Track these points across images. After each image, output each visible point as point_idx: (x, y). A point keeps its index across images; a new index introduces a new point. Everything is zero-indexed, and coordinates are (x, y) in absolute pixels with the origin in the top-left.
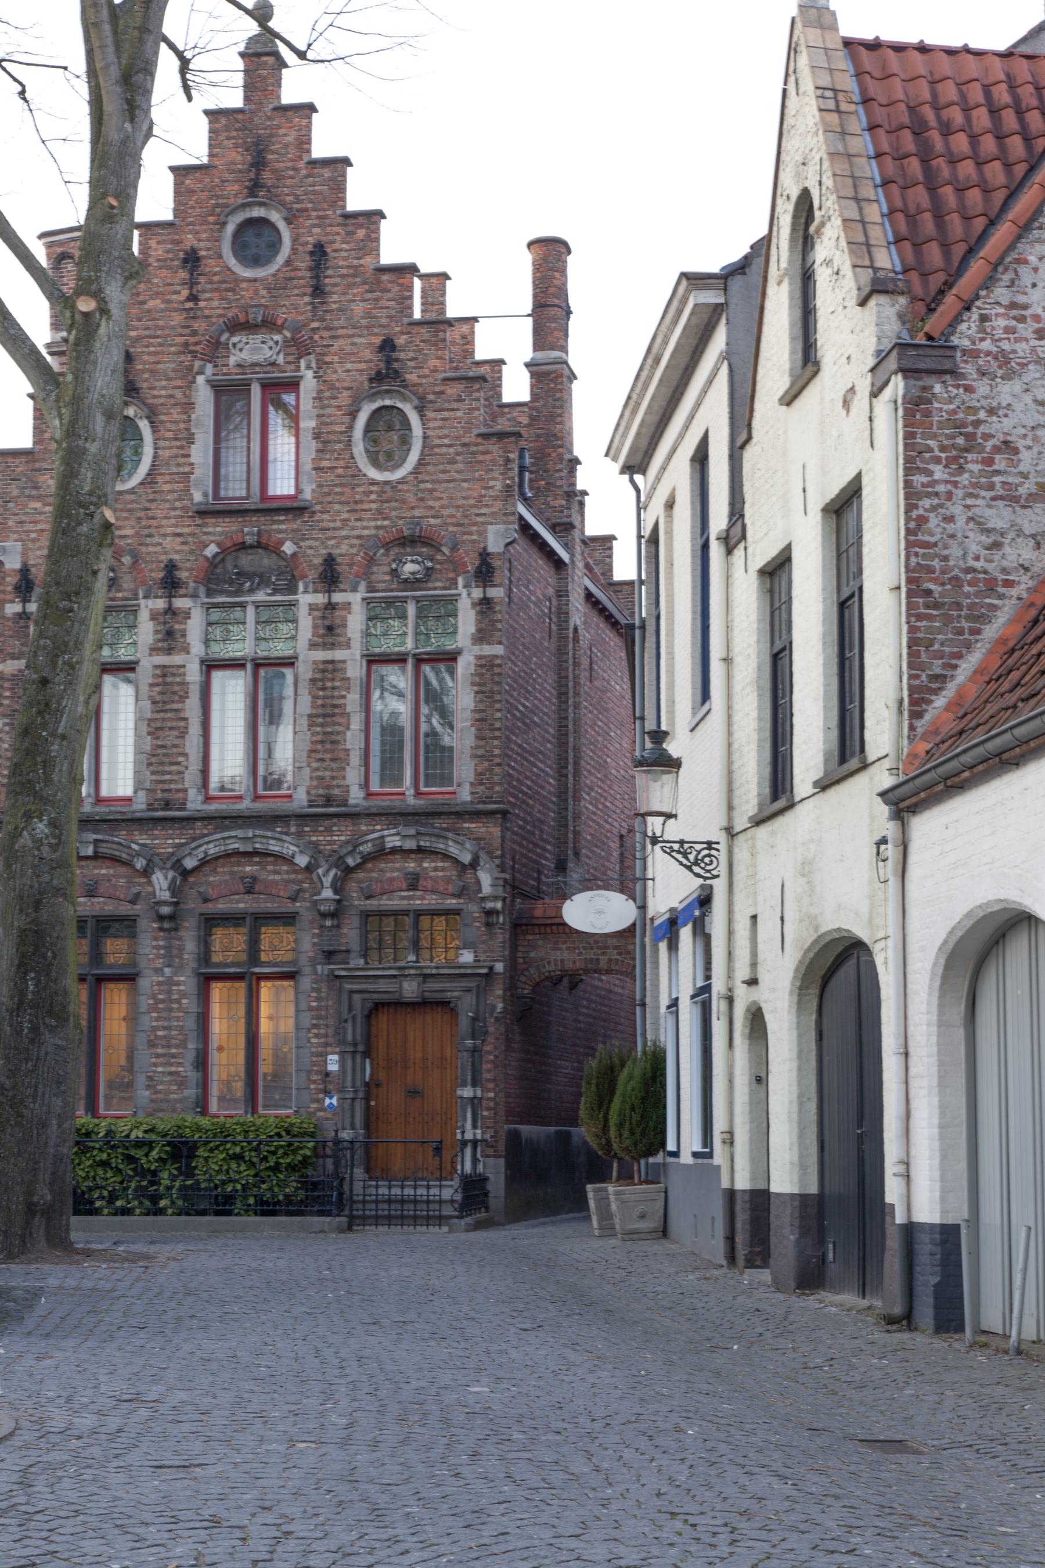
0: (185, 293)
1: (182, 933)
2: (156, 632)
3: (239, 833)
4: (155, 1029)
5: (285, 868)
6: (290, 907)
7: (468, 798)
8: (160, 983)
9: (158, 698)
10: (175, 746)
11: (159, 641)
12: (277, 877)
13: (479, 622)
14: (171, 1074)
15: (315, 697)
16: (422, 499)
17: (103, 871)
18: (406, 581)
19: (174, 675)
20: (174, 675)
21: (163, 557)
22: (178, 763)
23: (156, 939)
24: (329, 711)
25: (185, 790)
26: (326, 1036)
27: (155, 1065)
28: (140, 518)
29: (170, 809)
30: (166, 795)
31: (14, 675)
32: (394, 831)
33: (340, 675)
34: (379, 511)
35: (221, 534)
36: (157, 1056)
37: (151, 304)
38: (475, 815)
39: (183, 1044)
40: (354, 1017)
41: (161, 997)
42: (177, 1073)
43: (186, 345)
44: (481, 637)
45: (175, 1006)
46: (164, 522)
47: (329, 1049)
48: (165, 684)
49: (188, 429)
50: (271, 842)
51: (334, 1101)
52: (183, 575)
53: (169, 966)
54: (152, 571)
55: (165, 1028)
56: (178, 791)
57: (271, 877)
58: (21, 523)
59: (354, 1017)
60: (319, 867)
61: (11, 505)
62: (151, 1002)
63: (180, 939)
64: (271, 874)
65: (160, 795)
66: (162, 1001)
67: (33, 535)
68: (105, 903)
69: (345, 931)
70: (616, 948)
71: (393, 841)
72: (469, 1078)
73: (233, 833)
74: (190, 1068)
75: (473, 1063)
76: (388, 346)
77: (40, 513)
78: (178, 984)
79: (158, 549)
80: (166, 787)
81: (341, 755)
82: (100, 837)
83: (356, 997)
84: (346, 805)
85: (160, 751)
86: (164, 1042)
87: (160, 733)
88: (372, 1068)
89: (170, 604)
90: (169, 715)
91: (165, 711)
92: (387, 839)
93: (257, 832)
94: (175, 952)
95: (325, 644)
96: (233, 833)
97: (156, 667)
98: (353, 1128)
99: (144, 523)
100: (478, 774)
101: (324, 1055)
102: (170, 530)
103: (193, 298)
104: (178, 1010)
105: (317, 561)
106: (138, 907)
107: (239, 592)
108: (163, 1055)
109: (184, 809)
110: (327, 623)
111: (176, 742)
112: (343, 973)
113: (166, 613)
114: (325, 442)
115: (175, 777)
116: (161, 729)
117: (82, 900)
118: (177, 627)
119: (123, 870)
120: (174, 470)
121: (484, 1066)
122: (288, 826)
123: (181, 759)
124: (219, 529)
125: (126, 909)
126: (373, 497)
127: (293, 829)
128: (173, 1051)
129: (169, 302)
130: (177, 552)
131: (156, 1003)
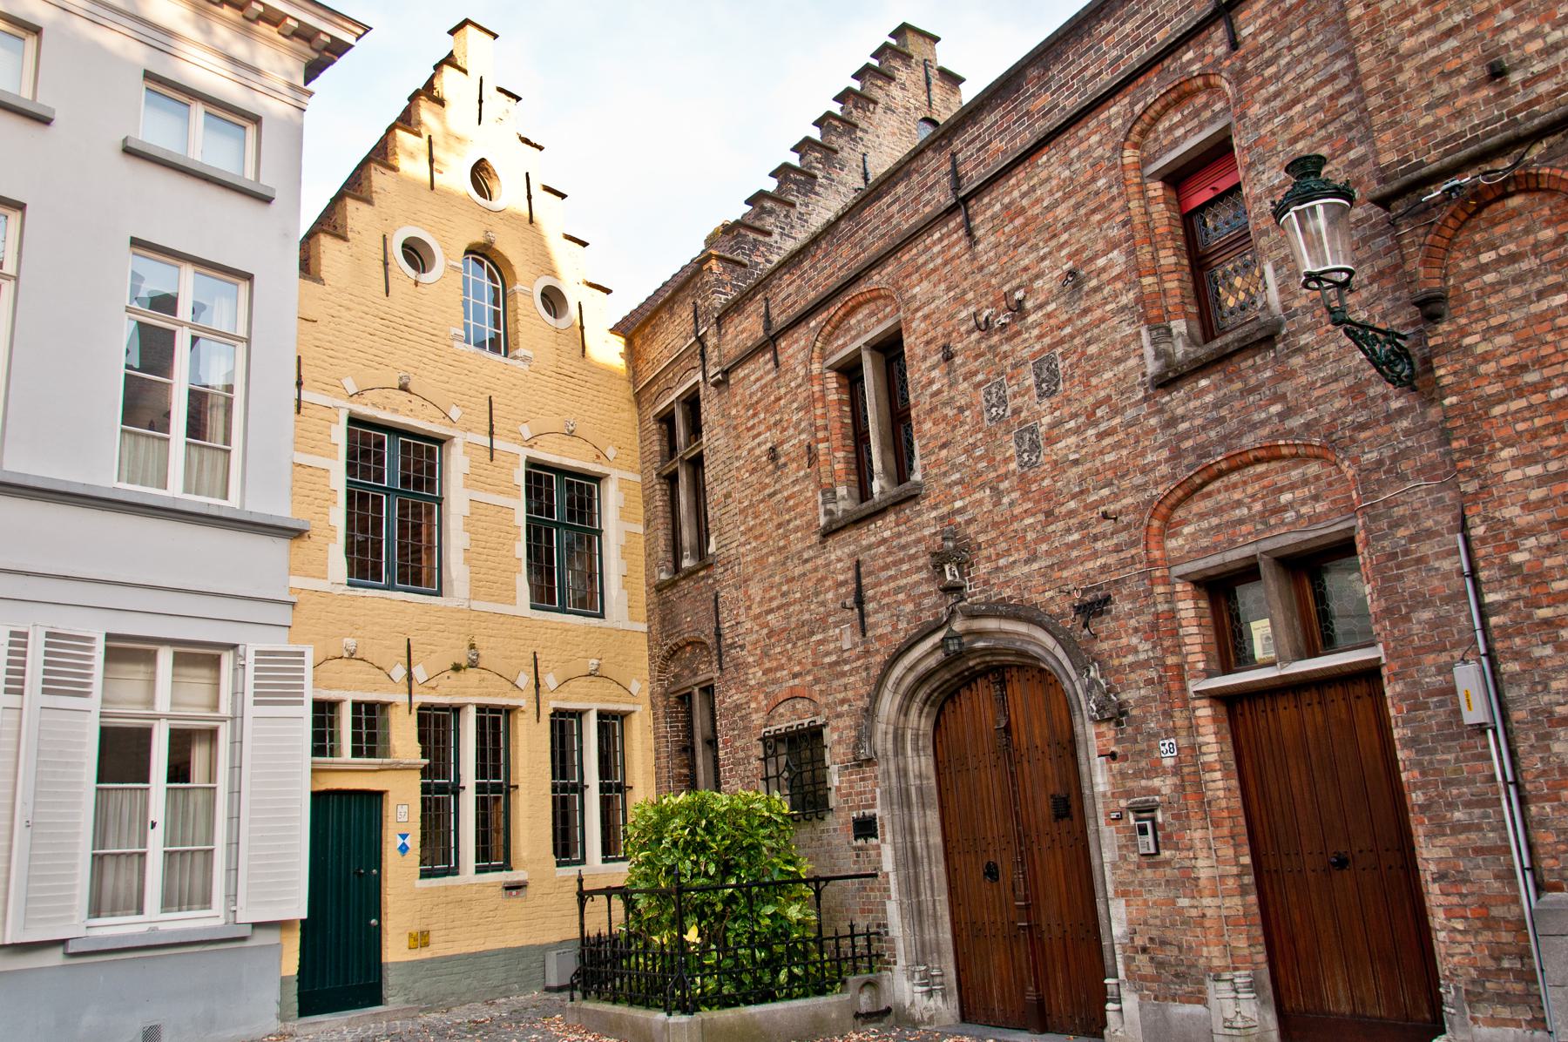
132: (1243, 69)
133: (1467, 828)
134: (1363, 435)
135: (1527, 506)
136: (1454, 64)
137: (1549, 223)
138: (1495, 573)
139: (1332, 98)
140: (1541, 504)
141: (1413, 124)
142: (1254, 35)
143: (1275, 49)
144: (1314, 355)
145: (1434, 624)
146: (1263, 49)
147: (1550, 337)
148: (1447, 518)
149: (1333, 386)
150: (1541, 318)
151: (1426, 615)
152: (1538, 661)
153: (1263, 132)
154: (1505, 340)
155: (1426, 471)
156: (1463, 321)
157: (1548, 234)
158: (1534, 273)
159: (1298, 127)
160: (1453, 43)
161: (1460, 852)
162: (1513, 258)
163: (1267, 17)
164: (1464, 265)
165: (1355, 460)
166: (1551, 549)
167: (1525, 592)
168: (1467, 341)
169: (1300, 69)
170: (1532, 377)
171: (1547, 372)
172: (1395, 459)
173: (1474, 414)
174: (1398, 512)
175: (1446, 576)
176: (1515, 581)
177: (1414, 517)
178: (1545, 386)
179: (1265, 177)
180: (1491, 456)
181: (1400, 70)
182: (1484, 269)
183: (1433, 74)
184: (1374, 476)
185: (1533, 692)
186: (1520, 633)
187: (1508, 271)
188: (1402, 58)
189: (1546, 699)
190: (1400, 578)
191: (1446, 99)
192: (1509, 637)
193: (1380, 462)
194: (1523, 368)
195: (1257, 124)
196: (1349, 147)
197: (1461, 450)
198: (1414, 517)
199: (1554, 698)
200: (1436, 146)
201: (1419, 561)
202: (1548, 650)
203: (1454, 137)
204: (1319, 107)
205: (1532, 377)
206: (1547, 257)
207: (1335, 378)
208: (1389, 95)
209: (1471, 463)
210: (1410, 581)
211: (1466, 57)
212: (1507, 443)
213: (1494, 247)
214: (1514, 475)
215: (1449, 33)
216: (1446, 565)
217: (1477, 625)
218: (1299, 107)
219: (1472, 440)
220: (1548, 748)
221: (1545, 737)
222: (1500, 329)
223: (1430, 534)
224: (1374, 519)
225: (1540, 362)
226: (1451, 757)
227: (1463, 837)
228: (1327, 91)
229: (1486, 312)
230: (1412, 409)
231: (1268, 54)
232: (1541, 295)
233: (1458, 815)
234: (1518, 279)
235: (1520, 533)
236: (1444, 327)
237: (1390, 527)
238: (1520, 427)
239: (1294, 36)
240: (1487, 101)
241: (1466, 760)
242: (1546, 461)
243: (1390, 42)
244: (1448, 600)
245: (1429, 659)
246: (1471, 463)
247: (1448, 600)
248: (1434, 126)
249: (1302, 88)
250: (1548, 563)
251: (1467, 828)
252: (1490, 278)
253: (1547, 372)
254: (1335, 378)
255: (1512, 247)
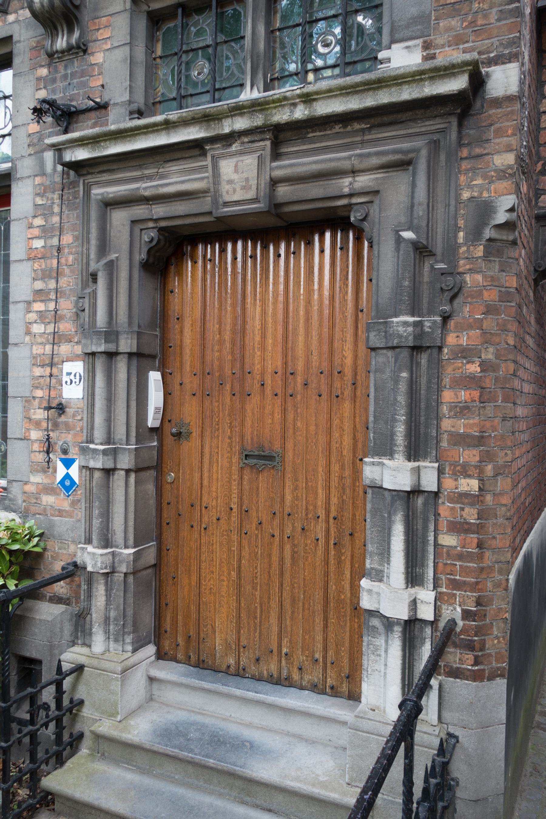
26: (57, 317)
40: (111, 266)
47: (64, 349)
51: (74, 471)
59: (111, 266)
69: (98, 58)
72: (400, 429)
75: (412, 384)
88: (167, 394)
98: (106, 543)
121: (448, 396)
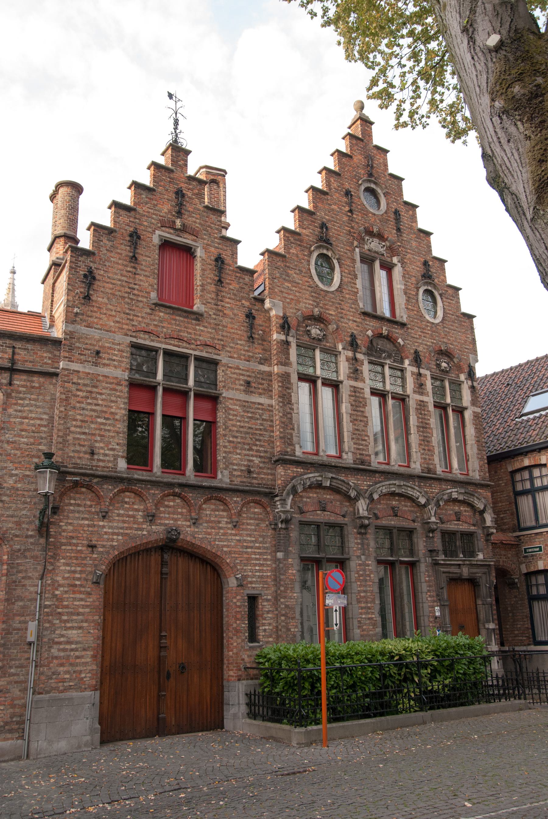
0: (347, 209)
1: (368, 536)
2: (349, 368)
3: (397, 482)
4: (359, 592)
5: (409, 504)
6: (412, 525)
7: (478, 478)
8: (360, 565)
9: (353, 403)
10: (363, 431)
11: (351, 373)
12: (406, 508)
13: (472, 396)
14: (369, 619)
15: (418, 417)
16: (446, 335)
17: (328, 497)
18: (443, 371)
19: (359, 393)
20: (359, 393)
21: (349, 330)
22: (365, 440)
23: (356, 539)
24: (424, 425)
25: (370, 456)
27: (361, 614)
28: (337, 308)
29: (364, 465)
30: (361, 457)
31: (282, 374)
32: (456, 490)
33: (426, 408)
34: (431, 335)
35: (373, 326)
36: (362, 608)
37: (333, 207)
38: (482, 486)
39: (373, 601)
41: (361, 573)
42: (372, 618)
43: (350, 231)
44: (474, 402)
45: (368, 578)
46: (348, 313)
48: (356, 396)
49: (354, 271)
50: (409, 489)
52: (359, 342)
53: (363, 555)
54: (345, 336)
55: (365, 591)
56: (367, 455)
57: (404, 508)
58: (282, 292)
60: (429, 504)
61: (275, 280)
62: (356, 575)
63: (367, 539)
64: (405, 507)
65: (359, 457)
66: (362, 575)
67: (288, 300)
68: (330, 516)
70: (504, 555)
71: (455, 495)
73: (394, 482)
74: (378, 615)
76: (425, 263)
77: (291, 290)
78: (368, 565)
79: (346, 325)
80: (361, 452)
81: (432, 448)
82: (334, 476)
83: (444, 575)
84: (436, 474)
85: (356, 432)
86: (364, 600)
87: (356, 422)
89: (355, 355)
90: (359, 413)
91: (357, 411)
92: (453, 494)
93: (405, 483)
94: (366, 547)
95: (419, 392)
96: (394, 482)
97: (351, 386)
99: (339, 310)
100: (481, 467)
101: (433, 607)
102: (351, 318)
103: (351, 211)
104: (370, 581)
105: (412, 351)
106: (346, 519)
107: (380, 357)
108: (365, 608)
109: (370, 466)
110: (419, 382)
111: (363, 428)
112: (442, 562)
113: (353, 359)
114: (409, 297)
115: (365, 448)
116: (357, 420)
117: (319, 512)
118: (358, 367)
119: (338, 497)
120: (350, 289)
122: (415, 481)
123: (366, 438)
124: (371, 324)
125: (340, 520)
126: (429, 328)
127: (417, 484)
128: (369, 605)
129: (341, 209)
130: (355, 330)
131: (359, 576)
132: (11, 394)
133: (14, 675)
134: (16, 539)
135: (64, 578)
136: (82, 443)
137: (90, 500)
138: (50, 596)
139: (39, 425)
140: (67, 578)
141: (68, 454)
142: (19, 386)
143: (25, 395)
144: (6, 505)
145: (23, 607)
146: (20, 393)
147: (82, 532)
148: (37, 575)
149: (10, 519)
150: (81, 525)
151: (21, 604)
152: (54, 624)
153: (11, 420)
154: (70, 528)
155: (34, 558)
156: (62, 517)
157: (88, 503)
158: (83, 512)
159: (25, 427)
160: (83, 437)
161: (9, 683)
162: (79, 505)
163: (25, 383)
164: (66, 501)
165: (11, 546)
166: (66, 592)
167: (56, 603)
168: (61, 524)
169: (31, 408)
170: (74, 541)
171: (79, 542)
172: (25, 550)
173: (57, 546)
174: (21, 568)
175: (31, 593)
176: (55, 599)
177: (26, 571)
178: (76, 545)
179: (7, 436)
180: (58, 560)
181: (69, 435)
182: (71, 505)
183: (77, 442)
184: (16, 554)
185: (51, 634)
186: (52, 615)
187: (77, 508)
188: (70, 431)
189: (53, 636)
190: (15, 589)
191: (78, 452)
192: (48, 616)
193: (19, 550)
194: (72, 538)
195: (10, 416)
196: (40, 444)
197: (50, 556)
198: (26, 571)
199: (56, 636)
200: (72, 464)
201: (24, 586)
202: (58, 622)
203: (77, 464)
204: (34, 425)
205: (74, 541)
206: (87, 509)
207: (12, 516)
208: (64, 440)
209: (52, 561)
210: (19, 592)
211: (86, 443)
212: (64, 558)
213: (75, 500)
214: (62, 568)
215: (84, 433)
216: (32, 589)
217: (38, 610)
218: (27, 421)
219: (54, 554)
220: (50, 651)
221: (50, 647)
222: (70, 524)
223: (30, 578)
224: (12, 568)
225: (78, 538)
226: (15, 651)
227: (12, 678)
228: (38, 422)
229: (68, 517)
230: (35, 537)
231: (21, 395)
232: (83, 519)
233: (12, 670)
234: (79, 512)
235: (60, 585)
236: (56, 517)
237: (17, 572)
238: (68, 554)
239: (33, 396)
240: (88, 459)
241: (20, 652)
242: (72, 566)
243: (69, 425)
244: (30, 600)
245: (17, 618)
246: (52, 561)
247: (30, 600)
248: (73, 457)
249: (30, 415)
250: (64, 596)
251: (14, 675)
252: (72, 508)
253: (79, 542)
254: (12, 516)
255: (79, 502)
